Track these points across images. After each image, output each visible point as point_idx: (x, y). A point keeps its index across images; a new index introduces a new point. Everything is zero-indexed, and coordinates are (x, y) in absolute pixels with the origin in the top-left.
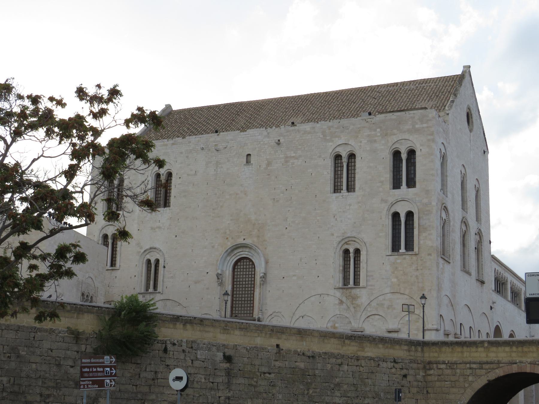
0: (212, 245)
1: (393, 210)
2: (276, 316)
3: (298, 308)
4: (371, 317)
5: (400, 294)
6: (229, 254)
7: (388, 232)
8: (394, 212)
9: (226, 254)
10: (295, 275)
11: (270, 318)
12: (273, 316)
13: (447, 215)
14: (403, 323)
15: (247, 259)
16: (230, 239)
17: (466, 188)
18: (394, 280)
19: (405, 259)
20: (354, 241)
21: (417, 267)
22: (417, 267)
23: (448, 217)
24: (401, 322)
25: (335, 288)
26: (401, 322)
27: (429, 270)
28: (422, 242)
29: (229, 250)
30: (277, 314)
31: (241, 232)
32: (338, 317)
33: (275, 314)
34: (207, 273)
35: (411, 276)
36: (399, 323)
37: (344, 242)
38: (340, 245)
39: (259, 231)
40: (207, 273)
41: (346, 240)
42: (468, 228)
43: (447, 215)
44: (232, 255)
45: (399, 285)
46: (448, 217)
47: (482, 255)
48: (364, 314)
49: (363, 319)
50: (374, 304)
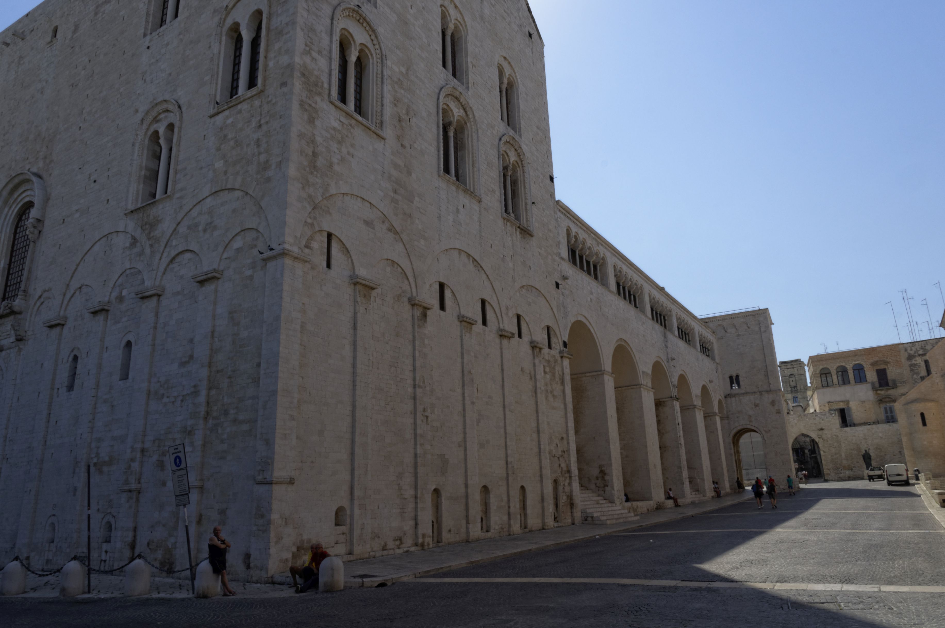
1: (229, 22)
3: (74, 273)
4: (177, 260)
5: (227, 192)
7: (218, 67)
8: (251, 40)
13: (375, 42)
14: (229, 258)
17: (466, 48)
18: (219, 165)
19: (240, 112)
20: (167, 111)
21: (260, 120)
22: (260, 120)
23: (377, 47)
24: (225, 255)
25: (125, 214)
26: (225, 255)
27: (281, 118)
28: (271, 64)
32: (127, 276)
35: (248, 145)
36: (221, 259)
37: (150, 118)
38: (145, 127)
41: (154, 114)
42: (471, 116)
43: (375, 42)
45: (226, 173)
46: (377, 47)
47: (525, 187)
48: (165, 255)
49: (162, 269)
50: (182, 229)
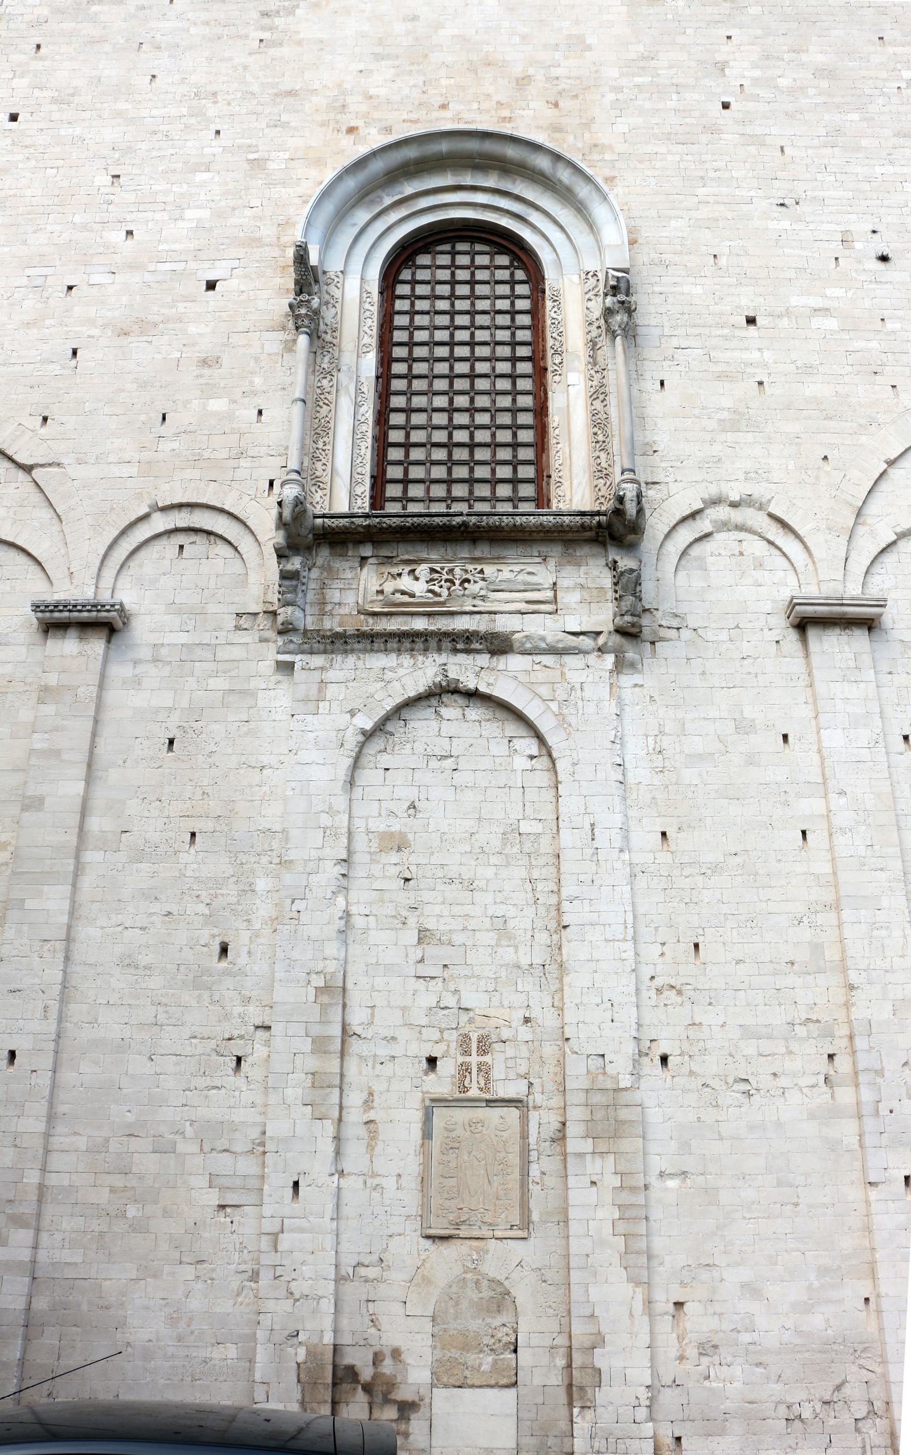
0: (252, 156)
2: (724, 526)
6: (363, 195)
9: (351, 184)
10: (827, 309)
11: (685, 535)
12: (704, 525)
15: (472, 240)
16: (374, 131)
29: (378, 166)
30: (737, 516)
31: (444, 107)
33: (722, 512)
34: (211, 286)
39: (556, 105)
40: (211, 286)
44: (388, 201)
